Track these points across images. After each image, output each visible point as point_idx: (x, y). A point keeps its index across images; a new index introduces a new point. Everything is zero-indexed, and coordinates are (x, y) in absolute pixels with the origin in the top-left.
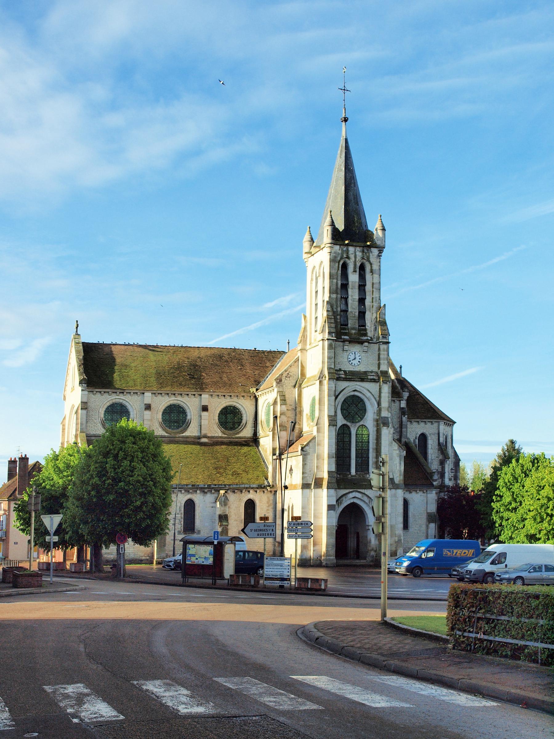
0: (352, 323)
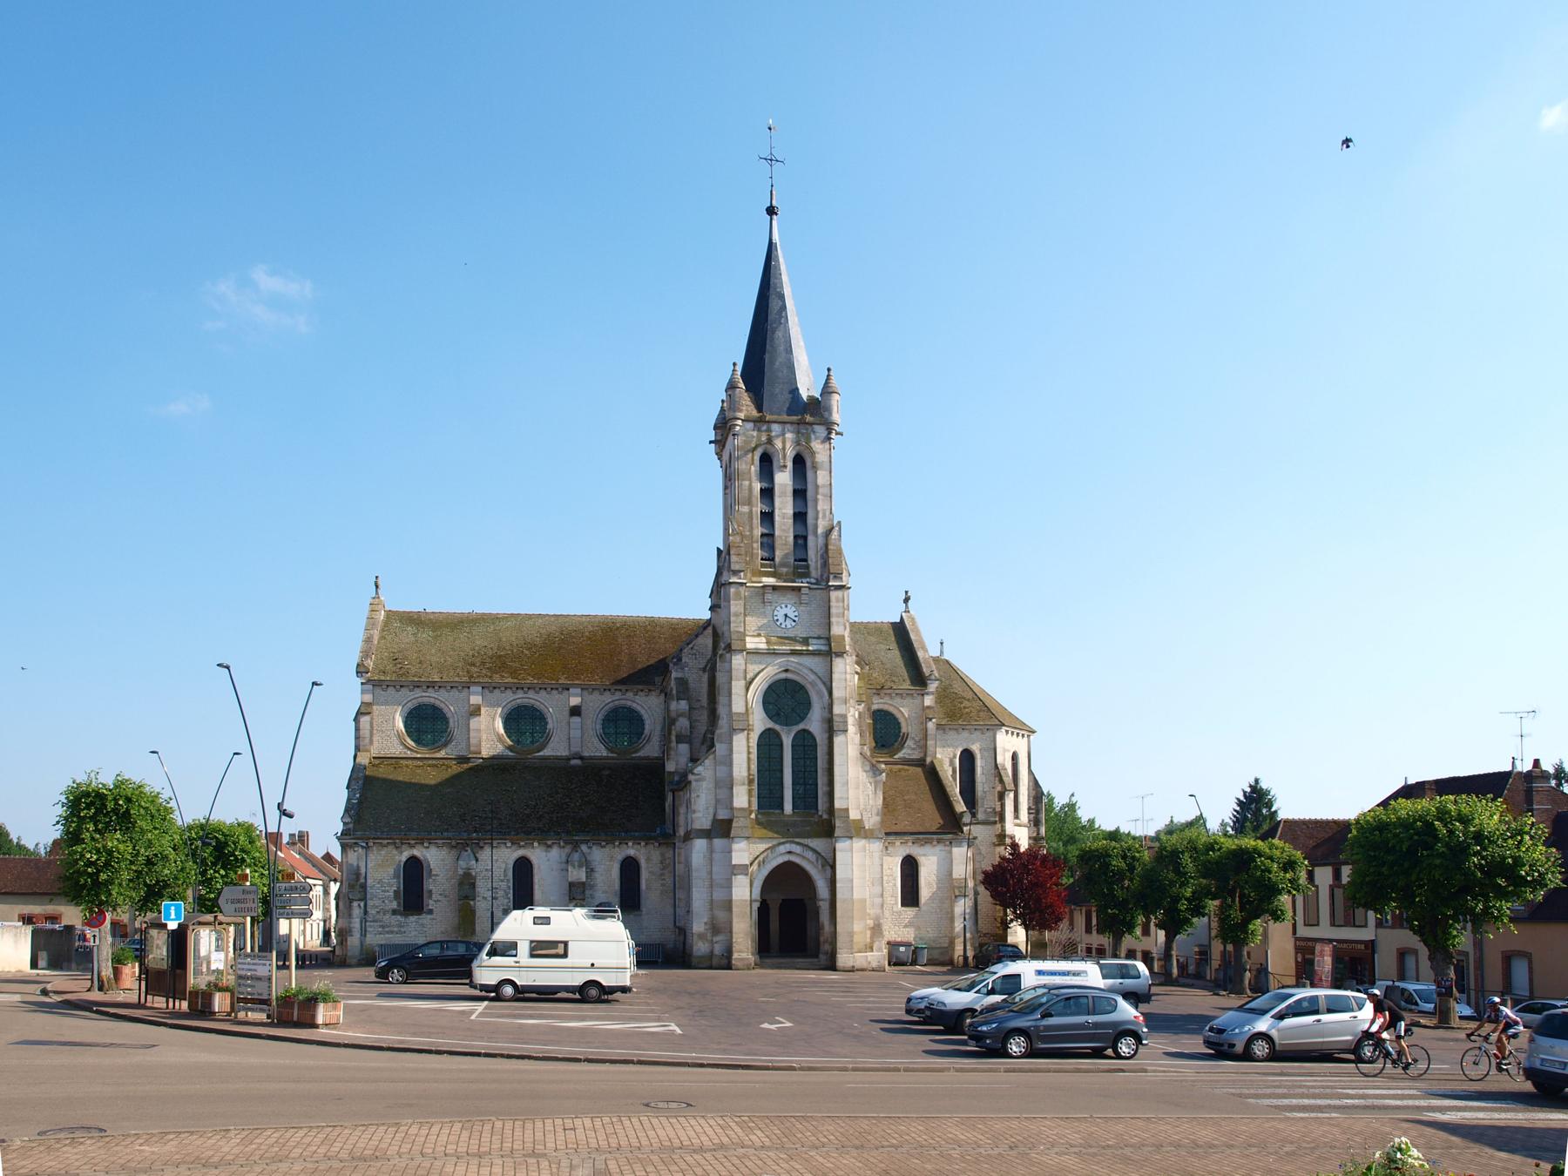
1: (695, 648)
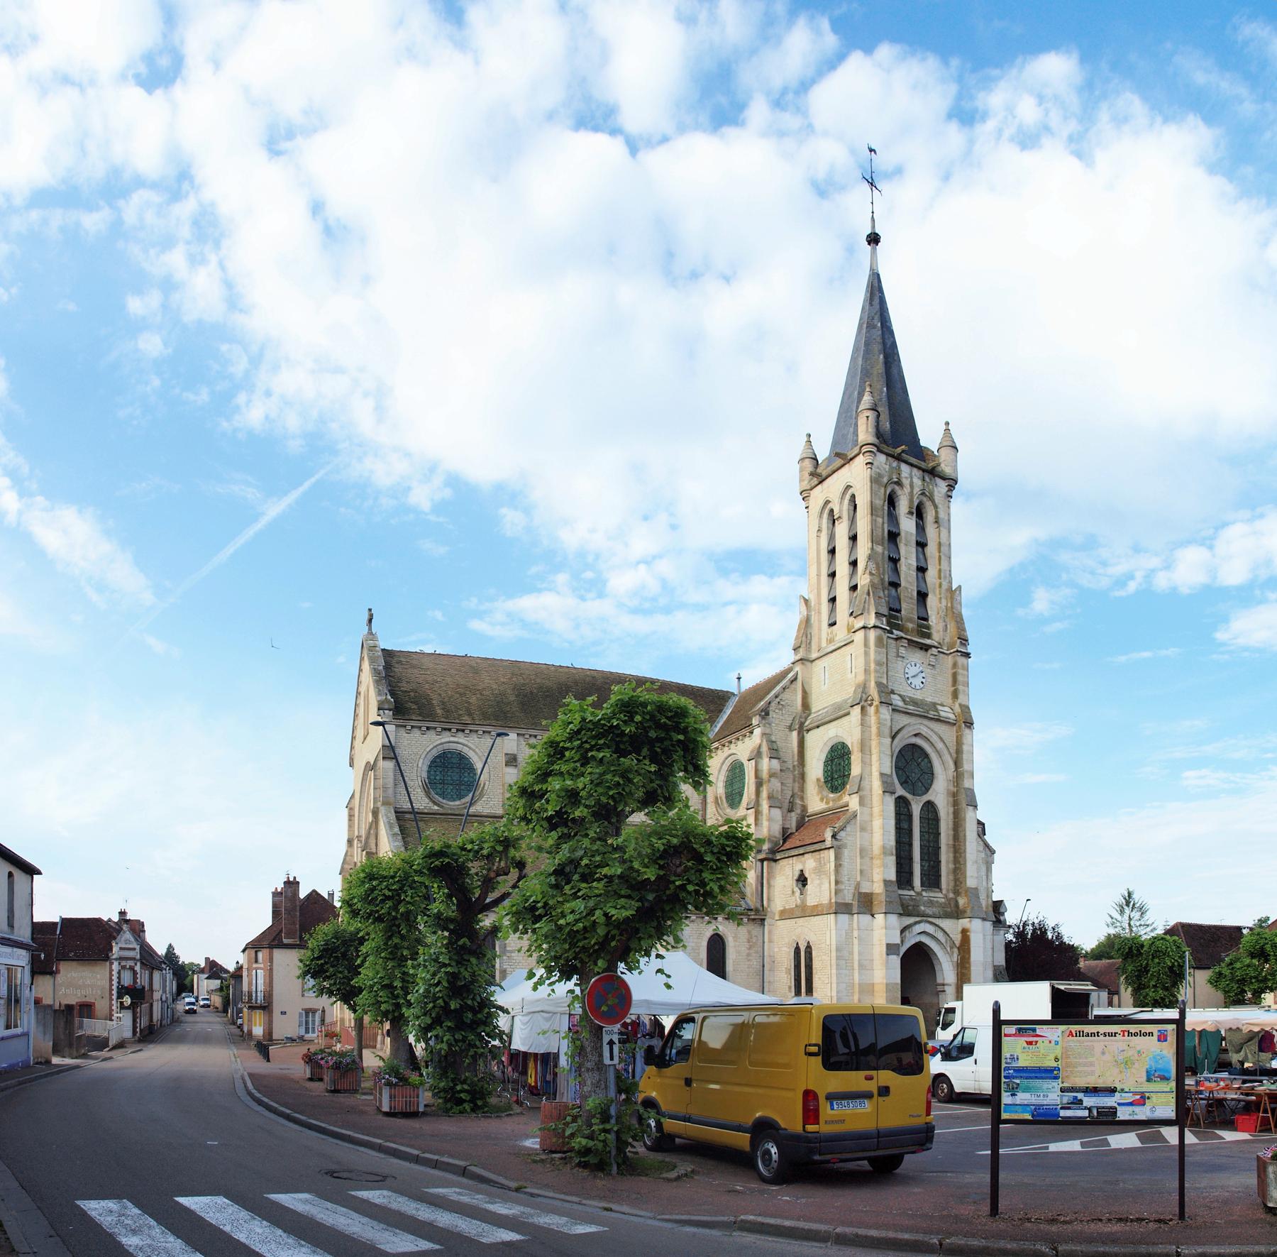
0: (908, 608)
1: (782, 703)
